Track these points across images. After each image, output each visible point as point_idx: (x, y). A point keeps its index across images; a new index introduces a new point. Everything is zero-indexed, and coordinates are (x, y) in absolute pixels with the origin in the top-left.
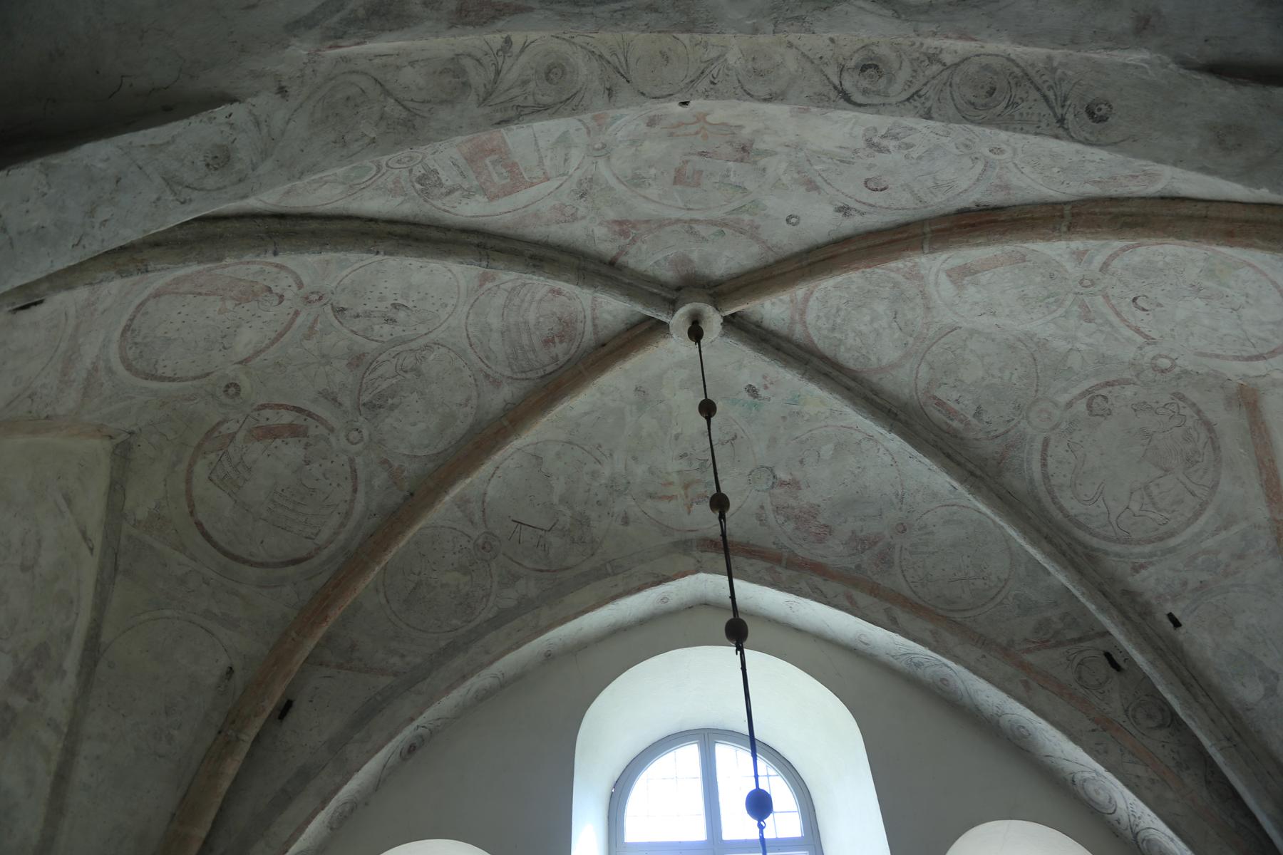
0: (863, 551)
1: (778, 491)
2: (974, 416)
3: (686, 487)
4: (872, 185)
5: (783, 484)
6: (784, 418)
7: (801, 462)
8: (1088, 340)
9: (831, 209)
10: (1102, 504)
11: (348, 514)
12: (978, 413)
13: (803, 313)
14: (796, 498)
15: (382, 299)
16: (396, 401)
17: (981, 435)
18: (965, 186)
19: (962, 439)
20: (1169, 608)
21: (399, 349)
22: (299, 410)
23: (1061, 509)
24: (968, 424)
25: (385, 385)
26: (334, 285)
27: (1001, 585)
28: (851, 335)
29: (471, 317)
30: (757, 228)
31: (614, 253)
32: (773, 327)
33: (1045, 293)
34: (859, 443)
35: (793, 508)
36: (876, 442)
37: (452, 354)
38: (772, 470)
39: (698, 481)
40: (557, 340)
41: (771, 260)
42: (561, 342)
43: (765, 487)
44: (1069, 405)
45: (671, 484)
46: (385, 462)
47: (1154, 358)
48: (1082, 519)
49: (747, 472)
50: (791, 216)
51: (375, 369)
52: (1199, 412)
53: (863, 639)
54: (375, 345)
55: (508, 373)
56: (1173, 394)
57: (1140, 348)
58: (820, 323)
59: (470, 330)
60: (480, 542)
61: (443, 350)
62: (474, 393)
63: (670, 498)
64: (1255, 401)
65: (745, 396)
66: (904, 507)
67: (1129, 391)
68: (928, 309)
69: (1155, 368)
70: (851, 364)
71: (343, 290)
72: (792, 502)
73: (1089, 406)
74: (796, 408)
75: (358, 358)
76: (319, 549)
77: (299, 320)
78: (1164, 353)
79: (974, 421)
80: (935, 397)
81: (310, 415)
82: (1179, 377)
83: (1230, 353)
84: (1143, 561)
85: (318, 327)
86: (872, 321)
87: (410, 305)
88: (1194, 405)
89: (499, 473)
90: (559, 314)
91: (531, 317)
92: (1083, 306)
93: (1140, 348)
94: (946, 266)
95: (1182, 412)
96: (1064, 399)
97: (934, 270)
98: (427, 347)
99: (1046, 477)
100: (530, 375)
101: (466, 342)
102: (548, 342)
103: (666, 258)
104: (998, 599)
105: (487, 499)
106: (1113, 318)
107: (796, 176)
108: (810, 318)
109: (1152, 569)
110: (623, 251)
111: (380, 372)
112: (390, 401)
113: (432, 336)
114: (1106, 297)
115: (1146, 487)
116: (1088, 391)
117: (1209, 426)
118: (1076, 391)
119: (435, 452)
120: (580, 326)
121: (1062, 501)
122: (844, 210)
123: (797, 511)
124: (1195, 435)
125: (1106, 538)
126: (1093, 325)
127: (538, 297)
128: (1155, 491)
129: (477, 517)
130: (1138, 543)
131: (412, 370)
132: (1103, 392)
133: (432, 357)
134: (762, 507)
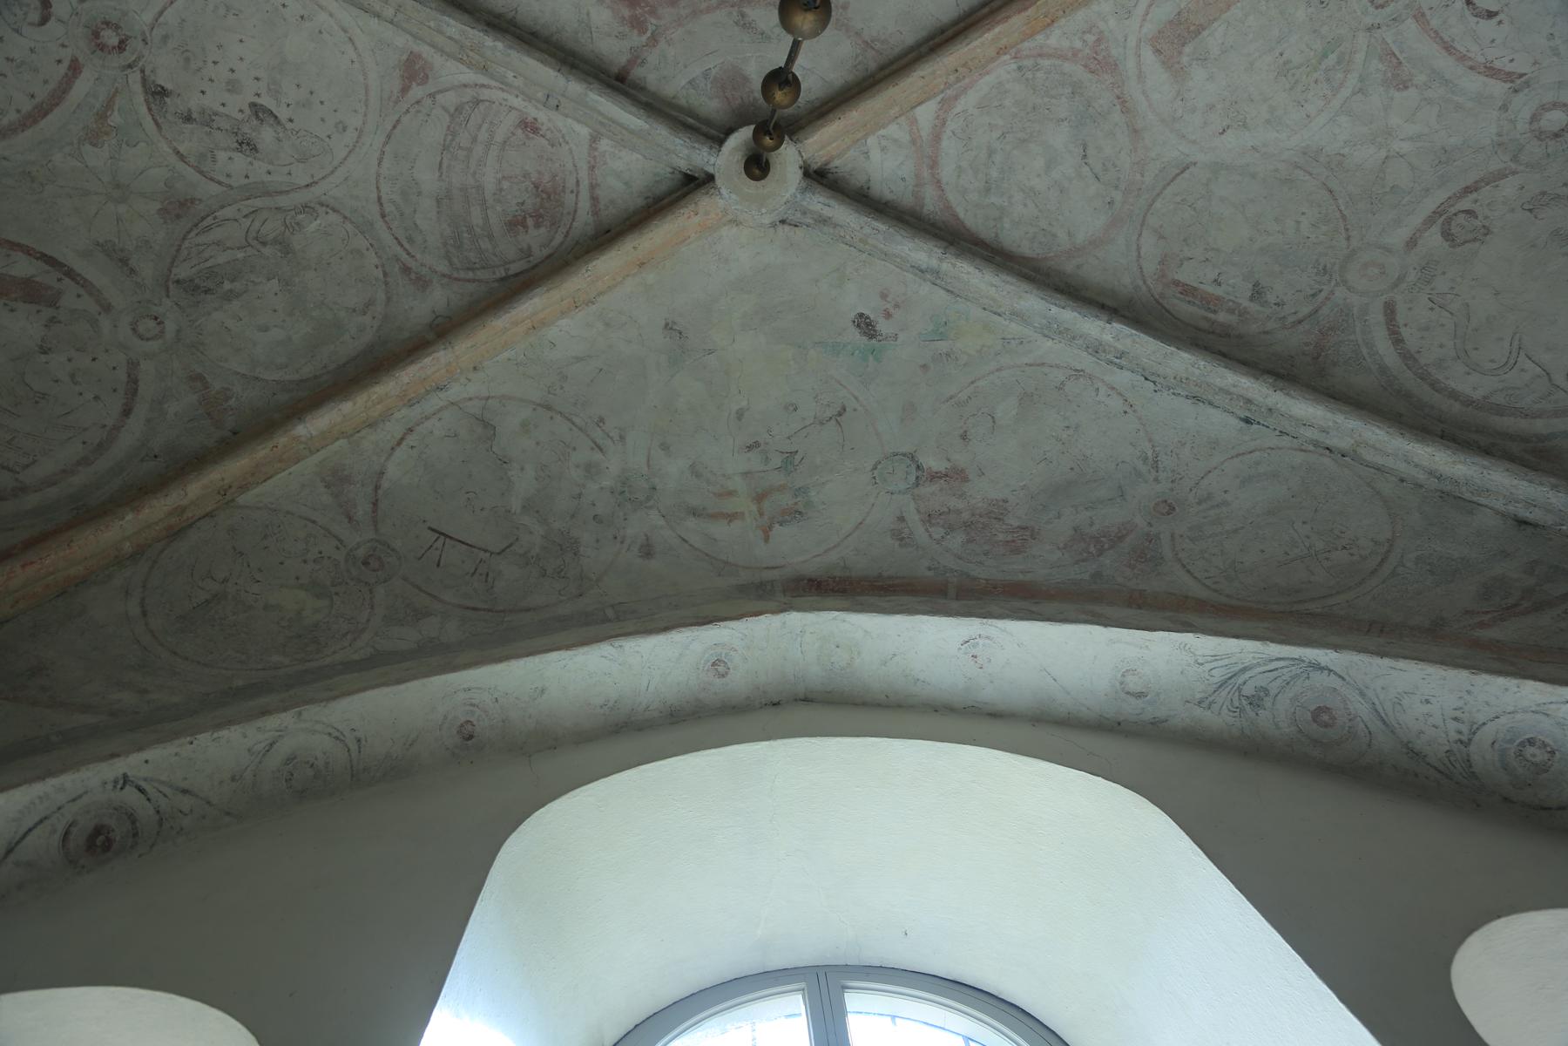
0: (1101, 552)
1: (927, 489)
2: (1252, 299)
3: (760, 498)
5: (934, 477)
6: (924, 367)
7: (964, 437)
10: (1529, 365)
11: (101, 448)
12: (1257, 293)
13: (934, 164)
14: (962, 496)
15: (233, 87)
16: (238, 286)
17: (1270, 325)
19: (1240, 337)
21: (258, 203)
22: (52, 262)
23: (1454, 395)
24: (1243, 313)
25: (222, 258)
26: (148, 17)
29: (386, 163)
31: (623, 60)
32: (888, 196)
35: (959, 512)
37: (349, 226)
38: (912, 457)
39: (782, 489)
40: (530, 222)
41: (873, 66)
42: (537, 226)
43: (902, 486)
44: (1412, 243)
45: (731, 493)
46: (199, 378)
47: (1534, 118)
48: (1499, 399)
51: (208, 228)
53: (1133, 684)
54: (214, 189)
55: (442, 267)
57: (1504, 108)
59: (385, 188)
60: (361, 552)
61: (333, 217)
62: (381, 296)
63: (731, 517)
65: (855, 336)
67: (1508, 188)
69: (1540, 135)
71: (165, 38)
72: (954, 503)
73: (1447, 235)
74: (943, 346)
75: (182, 204)
76: (23, 489)
77: (81, 87)
79: (1254, 307)
80: (1177, 283)
81: (71, 274)
85: (115, 119)
87: (283, 114)
89: (411, 440)
90: (534, 177)
91: (489, 182)
93: (1504, 108)
97: (1132, 42)
98: (306, 208)
99: (1408, 357)
100: (480, 274)
101: (375, 209)
102: (515, 224)
103: (706, 74)
105: (385, 484)
106: (1445, 63)
108: (947, 172)
110: (636, 58)
111: (216, 234)
112: (227, 286)
113: (317, 191)
114: (1420, 17)
116: (1437, 213)
118: (1417, 220)
119: (296, 377)
120: (569, 199)
121: (1452, 384)
123: (966, 516)
126: (1412, 93)
127: (499, 138)
129: (362, 510)
131: (275, 241)
132: (1466, 204)
133: (314, 226)
134: (902, 519)
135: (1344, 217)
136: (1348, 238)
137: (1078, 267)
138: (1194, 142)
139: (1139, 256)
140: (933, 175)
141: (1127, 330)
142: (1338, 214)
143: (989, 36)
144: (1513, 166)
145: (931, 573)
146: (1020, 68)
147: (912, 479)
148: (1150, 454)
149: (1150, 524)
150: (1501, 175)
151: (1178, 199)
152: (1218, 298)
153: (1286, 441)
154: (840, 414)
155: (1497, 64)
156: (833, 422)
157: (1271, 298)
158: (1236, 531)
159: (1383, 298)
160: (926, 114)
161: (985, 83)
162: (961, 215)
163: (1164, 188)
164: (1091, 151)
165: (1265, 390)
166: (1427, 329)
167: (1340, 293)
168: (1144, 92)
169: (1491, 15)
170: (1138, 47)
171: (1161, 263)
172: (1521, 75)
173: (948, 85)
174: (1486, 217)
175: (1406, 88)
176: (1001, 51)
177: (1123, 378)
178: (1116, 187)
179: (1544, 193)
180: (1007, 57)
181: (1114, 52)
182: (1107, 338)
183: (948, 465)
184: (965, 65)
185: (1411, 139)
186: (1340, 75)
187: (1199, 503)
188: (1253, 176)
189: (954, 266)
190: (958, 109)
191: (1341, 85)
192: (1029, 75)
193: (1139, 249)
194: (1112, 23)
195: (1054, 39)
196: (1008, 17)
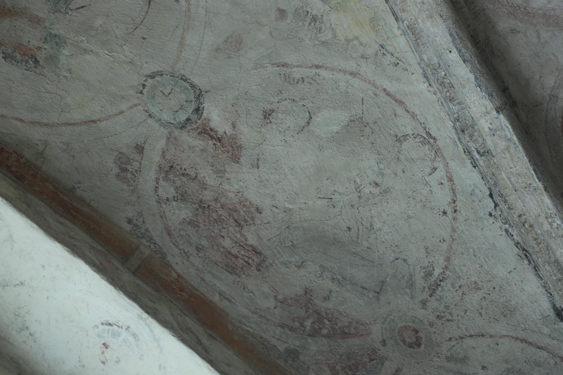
0: (315, 333)
1: (188, 139)
5: (207, 132)
6: (282, 13)
7: (267, 115)
14: (220, 172)
34: (400, 139)
35: (204, 186)
36: (438, 152)
38: (199, 95)
39: (36, 21)
43: (166, 117)
49: (147, 72)
66: (433, 303)
72: (206, 174)
123: (208, 196)
134: (140, 149)
137: (513, 31)
141: (509, 132)
145: (128, 227)
147: (183, 117)
148: (437, 272)
177: (469, 177)
182: (484, 125)
183: (228, 129)
187: (448, 359)
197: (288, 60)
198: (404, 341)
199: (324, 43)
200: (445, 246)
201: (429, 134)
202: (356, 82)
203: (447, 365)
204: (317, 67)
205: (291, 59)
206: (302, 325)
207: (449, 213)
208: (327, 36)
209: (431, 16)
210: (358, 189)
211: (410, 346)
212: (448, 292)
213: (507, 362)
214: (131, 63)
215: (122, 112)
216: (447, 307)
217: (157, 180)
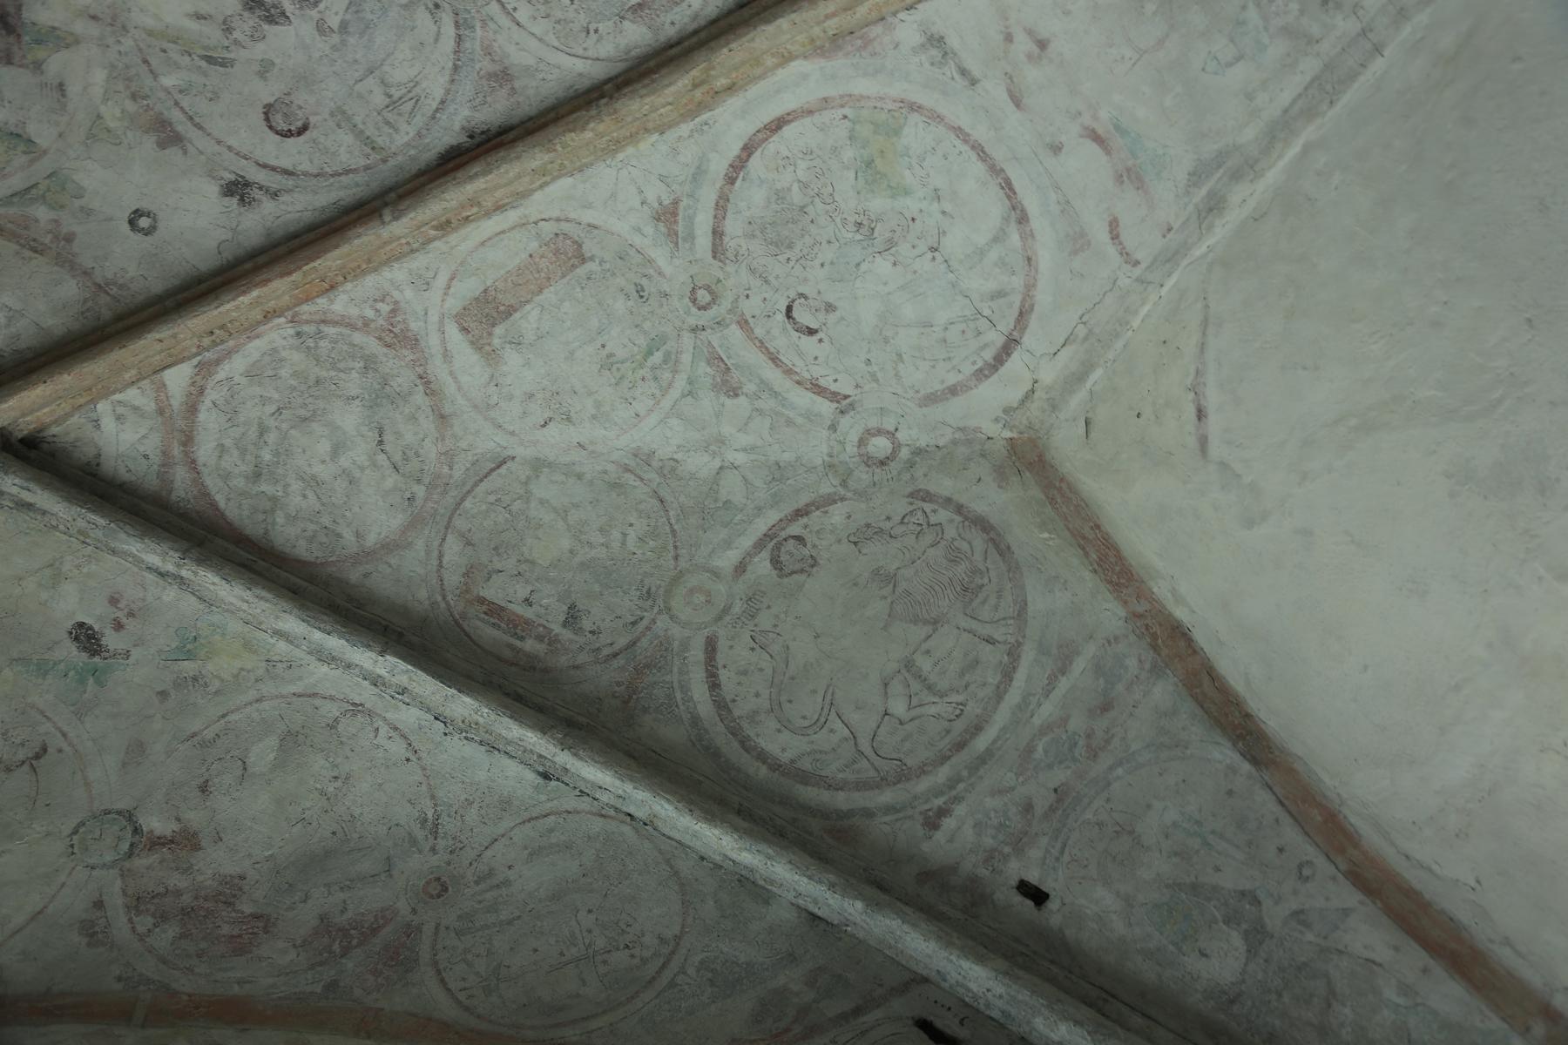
0: (345, 952)
2: (565, 624)
4: (279, 122)
5: (157, 843)
6: (163, 694)
8: (744, 440)
9: (213, 189)
10: (839, 725)
12: (572, 618)
13: (188, 440)
14: (188, 870)
17: (582, 658)
18: (438, 93)
19: (546, 671)
20: (1016, 870)
23: (762, 756)
24: (553, 641)
27: (666, 950)
28: (296, 486)
30: (69, 238)
32: (124, 476)
33: (642, 342)
34: (333, 726)
35: (178, 893)
36: (371, 714)
38: (129, 816)
41: (107, 314)
43: (109, 857)
44: (741, 568)
47: (862, 442)
48: (806, 764)
49: (67, 830)
50: (138, 213)
52: (959, 509)
56: (911, 495)
57: (833, 427)
58: (226, 463)
64: (1041, 457)
65: (71, 652)
66: (441, 843)
67: (837, 515)
68: (442, 418)
69: (868, 461)
70: (302, 550)
72: (177, 881)
73: (776, 562)
74: (189, 667)
78: (873, 423)
79: (566, 634)
80: (482, 600)
82: (911, 465)
83: (968, 369)
84: (939, 802)
86: (336, 452)
88: (949, 500)
92: (715, 359)
94: (454, 304)
95: (933, 520)
96: (726, 561)
97: (434, 318)
99: (722, 706)
104: (667, 975)
107: (131, 107)
108: (205, 451)
109: (960, 810)
114: (743, 323)
115: (909, 665)
116: (768, 536)
117: (982, 524)
118: (747, 542)
121: (763, 743)
122: (238, 189)
123: (186, 899)
124: (965, 546)
125: (862, 786)
126: (742, 400)
128: (925, 664)
130: (922, 771)
132: (795, 529)
134: (99, 905)
135: (674, 532)
136: (676, 558)
137: (366, 575)
138: (512, 433)
139: (440, 565)
140: (186, 453)
141: (403, 665)
142: (668, 528)
143: (244, 300)
144: (842, 491)
145: (119, 986)
146: (298, 334)
147: (125, 847)
148: (430, 815)
149: (414, 911)
150: (831, 500)
151: (492, 498)
152: (527, 622)
153: (585, 804)
154: (37, 757)
155: (822, 382)
156: (26, 768)
157: (587, 624)
158: (510, 923)
159: (706, 632)
160: (178, 379)
161: (255, 349)
162: (222, 505)
163: (476, 485)
164: (388, 437)
165: (551, 747)
166: (745, 673)
167: (662, 623)
168: (451, 373)
169: (811, 332)
170: (441, 322)
171: (466, 575)
172: (846, 397)
173: (201, 350)
174: (814, 546)
175: (737, 395)
176: (268, 316)
177: (410, 716)
178: (419, 481)
179: (868, 526)
180: (282, 320)
181: (413, 326)
182: (383, 672)
183: (175, 826)
184: (222, 327)
185: (745, 450)
186: (667, 375)
187: (477, 883)
188: (580, 477)
189: (196, 574)
190: (222, 373)
191: (670, 385)
192: (311, 343)
193: (441, 556)
194: (409, 293)
195: (339, 304)
196: (269, 280)
197: (195, 729)
198: (432, 897)
199: (216, 693)
200: (424, 788)
201: (354, 704)
202: (266, 705)
203: (477, 889)
204: (224, 716)
205: (196, 726)
206: (330, 952)
207: (413, 758)
208: (217, 684)
209: (277, 617)
210: (323, 793)
211: (439, 896)
212: (449, 825)
213: (526, 848)
214: (48, 834)
215: (63, 885)
216: (454, 838)
217: (130, 921)
